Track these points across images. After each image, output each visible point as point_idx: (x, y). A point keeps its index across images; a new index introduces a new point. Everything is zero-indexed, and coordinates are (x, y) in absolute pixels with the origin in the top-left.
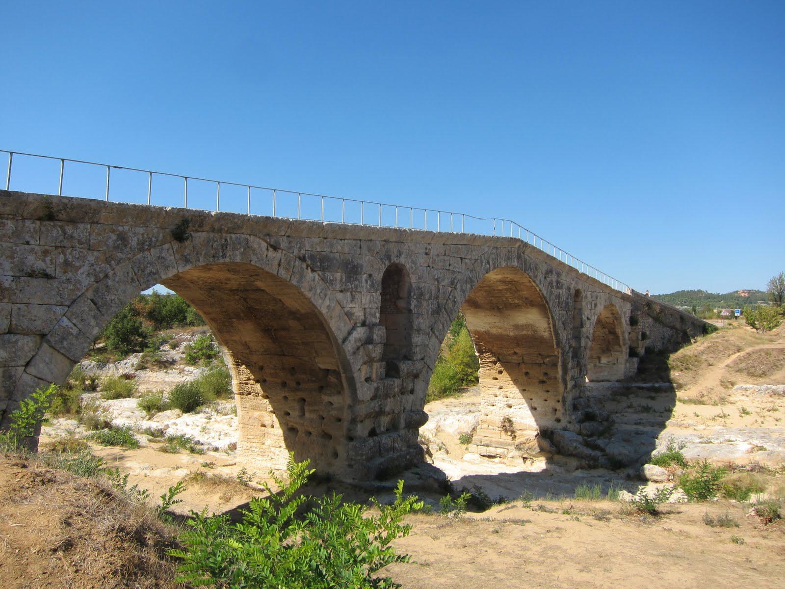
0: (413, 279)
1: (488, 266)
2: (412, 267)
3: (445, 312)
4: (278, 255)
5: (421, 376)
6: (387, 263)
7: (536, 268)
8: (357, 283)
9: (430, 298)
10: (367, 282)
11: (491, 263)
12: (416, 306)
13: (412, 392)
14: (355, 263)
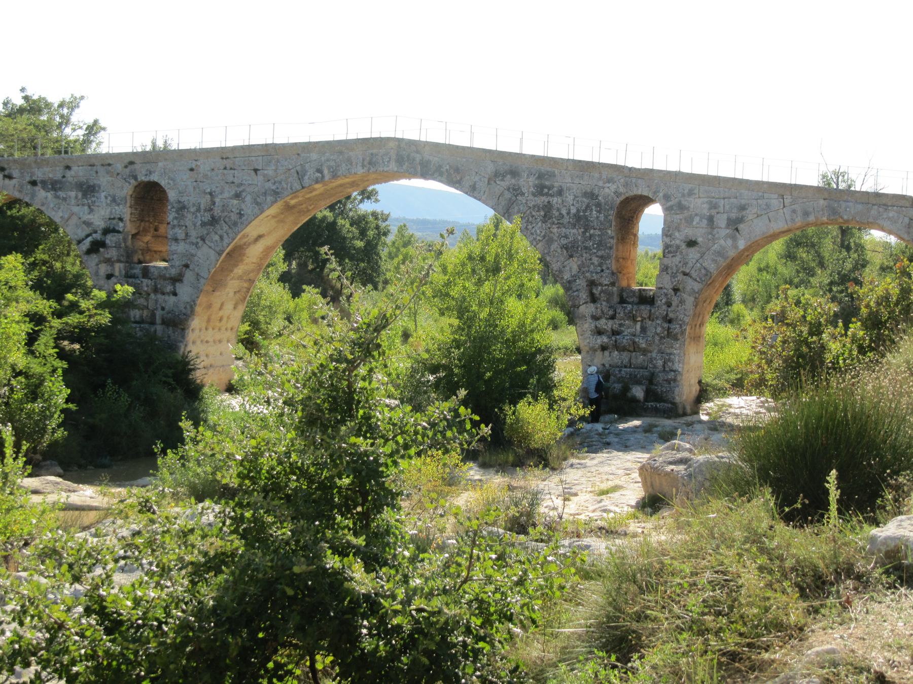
0: (172, 195)
1: (319, 175)
2: (169, 183)
3: (224, 224)
4: (14, 181)
5: (185, 280)
6: (133, 181)
7: (457, 170)
8: (93, 199)
9: (199, 210)
10: (106, 198)
11: (326, 172)
12: (176, 218)
13: (175, 294)
14: (92, 184)
